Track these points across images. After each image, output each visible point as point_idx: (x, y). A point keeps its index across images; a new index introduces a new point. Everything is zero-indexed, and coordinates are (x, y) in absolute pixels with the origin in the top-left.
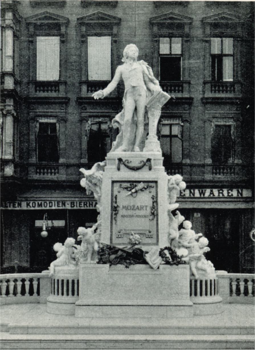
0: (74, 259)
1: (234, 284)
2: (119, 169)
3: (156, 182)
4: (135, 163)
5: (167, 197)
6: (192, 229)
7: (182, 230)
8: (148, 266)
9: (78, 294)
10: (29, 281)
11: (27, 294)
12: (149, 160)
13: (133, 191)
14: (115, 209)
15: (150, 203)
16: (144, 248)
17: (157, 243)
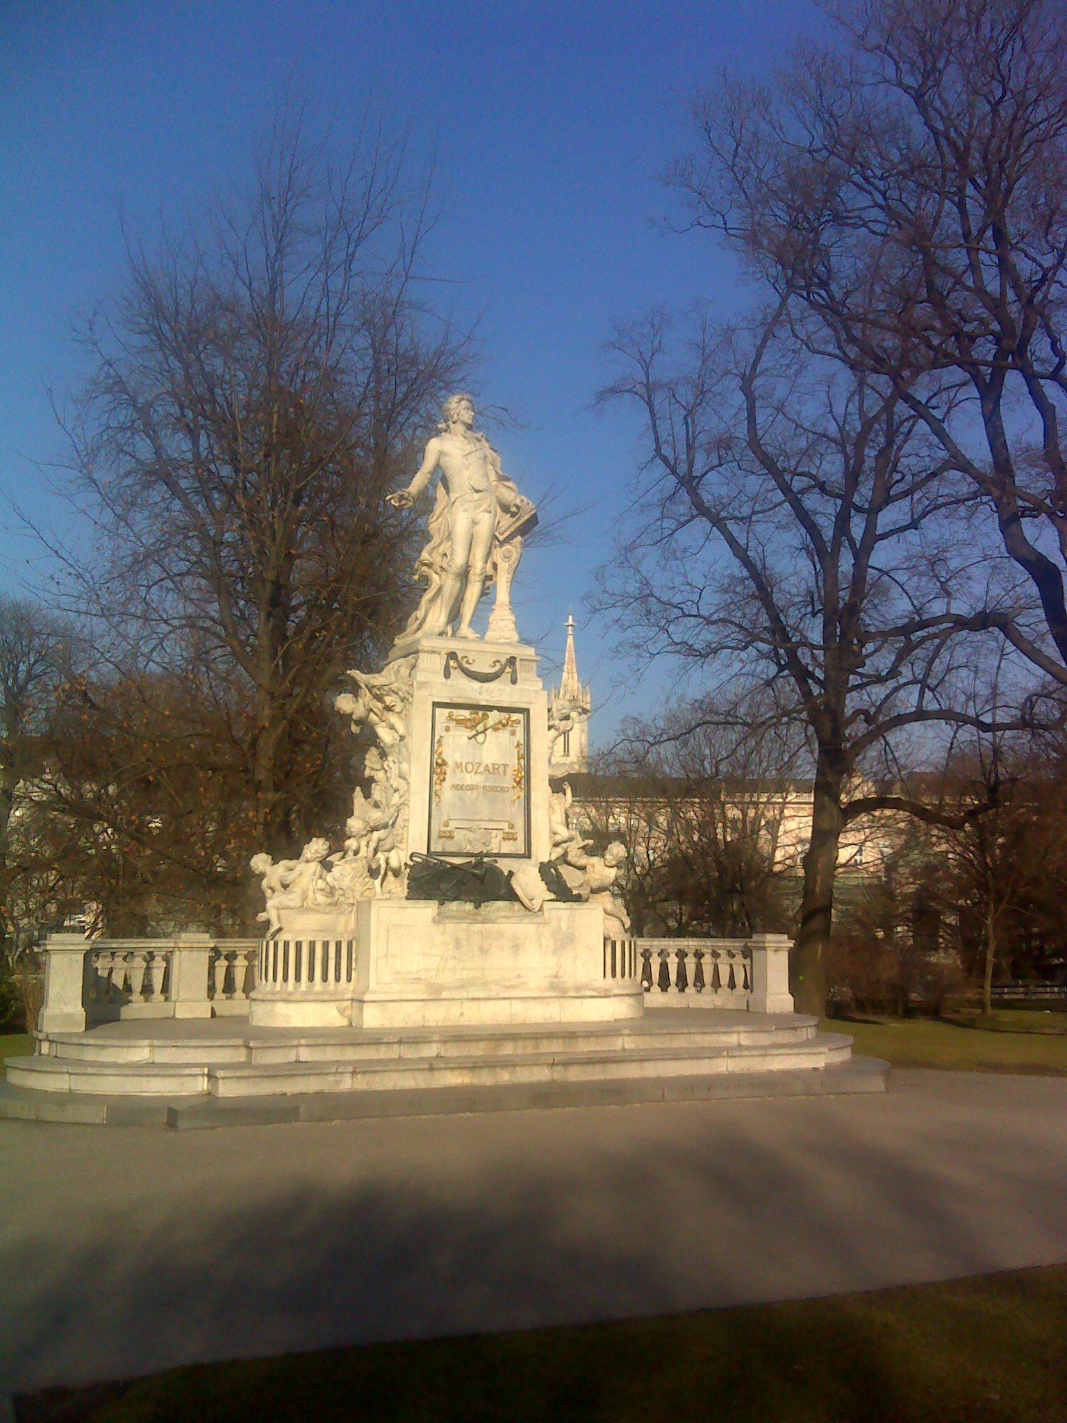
2: (447, 675)
3: (526, 712)
8: (517, 906)
10: (144, 959)
12: (512, 661)
13: (480, 727)
14: (437, 768)
15: (513, 762)
16: (504, 865)
17: (527, 855)
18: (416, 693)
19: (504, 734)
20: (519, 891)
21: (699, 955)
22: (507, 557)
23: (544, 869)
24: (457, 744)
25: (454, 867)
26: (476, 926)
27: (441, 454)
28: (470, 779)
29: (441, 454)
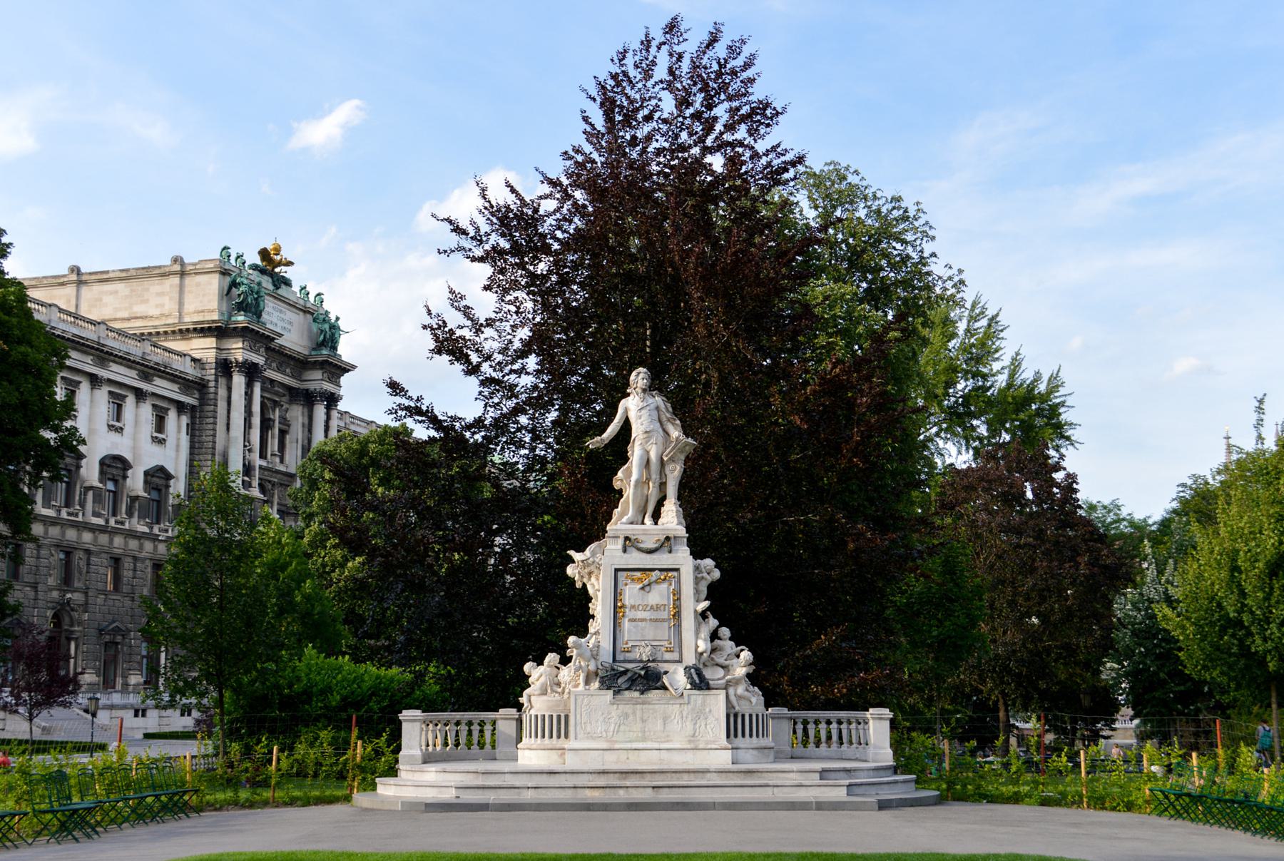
1: (800, 727)
2: (625, 551)
6: (731, 639)
7: (717, 642)
9: (566, 736)
12: (668, 538)
16: (663, 667)
19: (665, 585)
25: (626, 671)
26: (639, 707)
27: (626, 410)
28: (640, 615)
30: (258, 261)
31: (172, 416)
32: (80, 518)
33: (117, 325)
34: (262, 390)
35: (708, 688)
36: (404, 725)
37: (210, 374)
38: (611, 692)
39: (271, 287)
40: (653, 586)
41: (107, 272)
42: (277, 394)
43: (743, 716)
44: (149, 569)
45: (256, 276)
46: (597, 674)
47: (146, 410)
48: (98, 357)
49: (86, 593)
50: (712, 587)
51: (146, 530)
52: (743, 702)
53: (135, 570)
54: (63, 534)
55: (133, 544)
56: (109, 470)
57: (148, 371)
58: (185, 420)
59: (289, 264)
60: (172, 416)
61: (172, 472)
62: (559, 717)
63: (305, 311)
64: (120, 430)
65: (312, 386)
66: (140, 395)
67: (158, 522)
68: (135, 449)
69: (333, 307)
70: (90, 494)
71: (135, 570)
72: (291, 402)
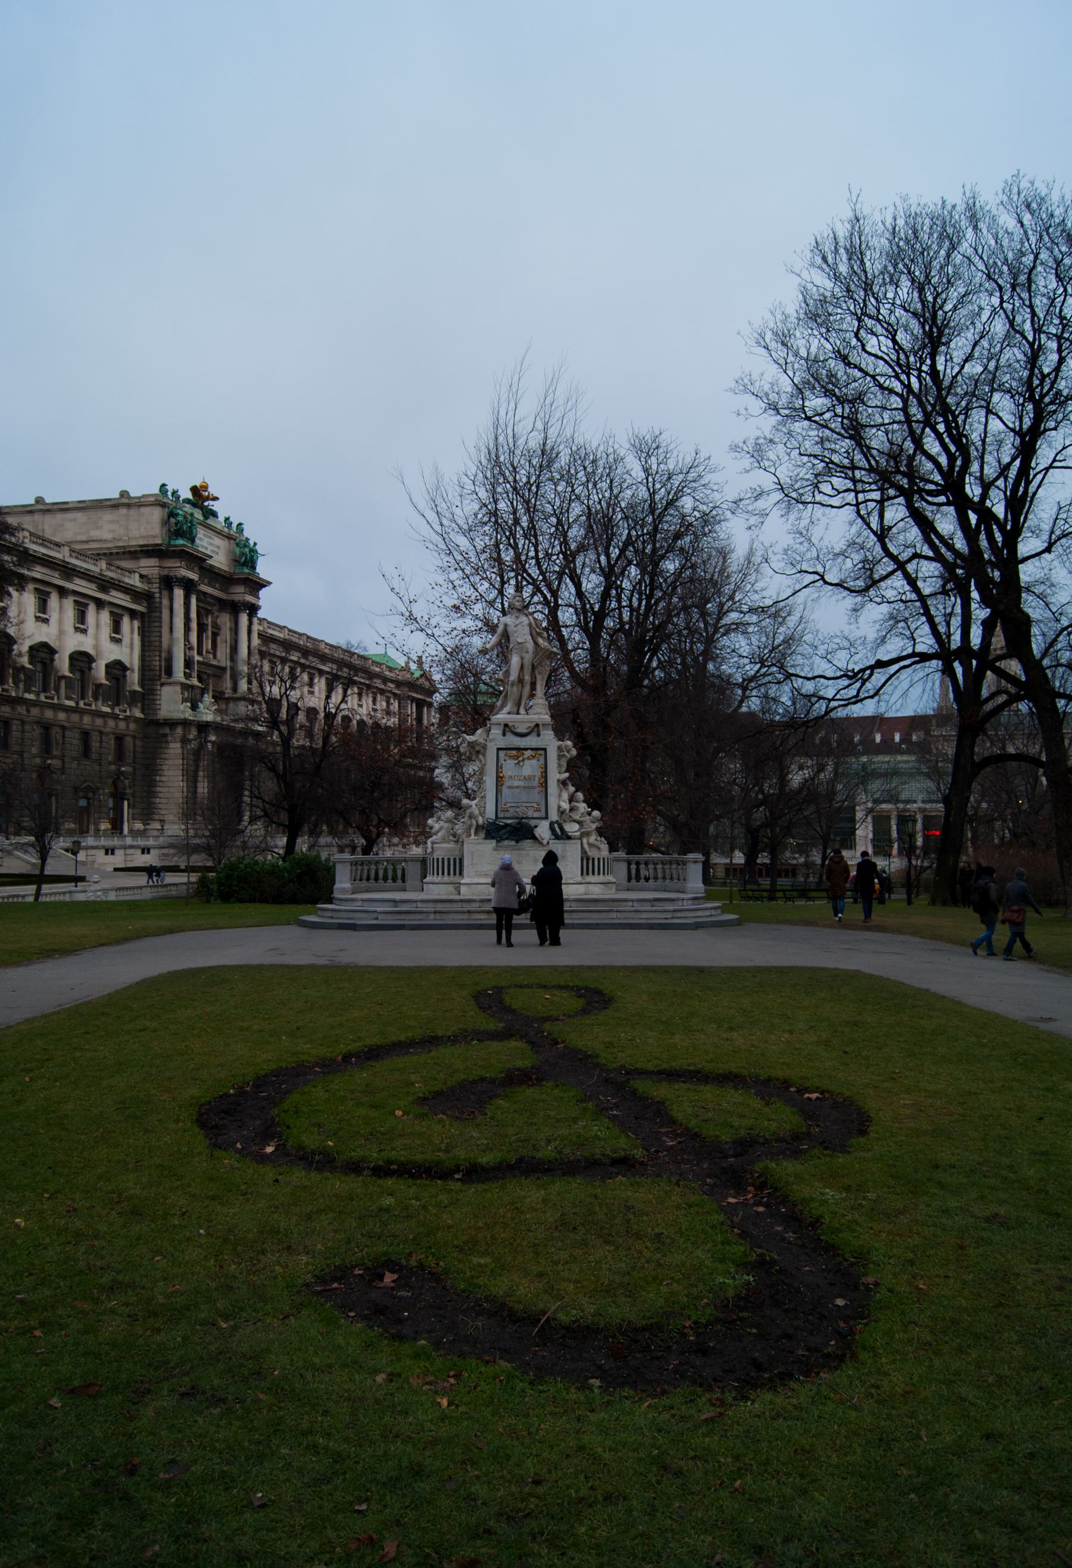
0: (454, 835)
1: (633, 867)
2: (504, 735)
3: (545, 750)
4: (522, 729)
5: (556, 765)
6: (584, 801)
11: (390, 881)
12: (537, 725)
14: (499, 780)
15: (538, 773)
16: (533, 823)
18: (489, 744)
19: (534, 762)
20: (537, 835)
21: (638, 864)
22: (540, 673)
23: (551, 825)
24: (509, 767)
25: (507, 825)
27: (506, 625)
28: (516, 783)
29: (506, 625)
30: (191, 497)
31: (126, 621)
32: (56, 701)
33: (78, 547)
34: (198, 600)
35: (569, 838)
36: (338, 866)
37: (155, 588)
38: (494, 842)
39: (201, 518)
40: (526, 762)
41: (67, 503)
42: (209, 604)
43: (593, 859)
44: (113, 741)
45: (188, 508)
46: (483, 827)
47: (105, 617)
48: (64, 572)
49: (63, 760)
50: (569, 763)
51: (108, 710)
52: (593, 849)
53: (101, 742)
54: (42, 713)
55: (99, 721)
56: (77, 663)
57: (105, 585)
58: (136, 624)
59: (216, 499)
60: (126, 621)
61: (128, 665)
62: (455, 860)
63: (229, 537)
64: (84, 631)
65: (236, 598)
66: (100, 604)
67: (118, 704)
68: (96, 646)
69: (251, 533)
70: (63, 683)
71: (101, 742)
72: (220, 611)
